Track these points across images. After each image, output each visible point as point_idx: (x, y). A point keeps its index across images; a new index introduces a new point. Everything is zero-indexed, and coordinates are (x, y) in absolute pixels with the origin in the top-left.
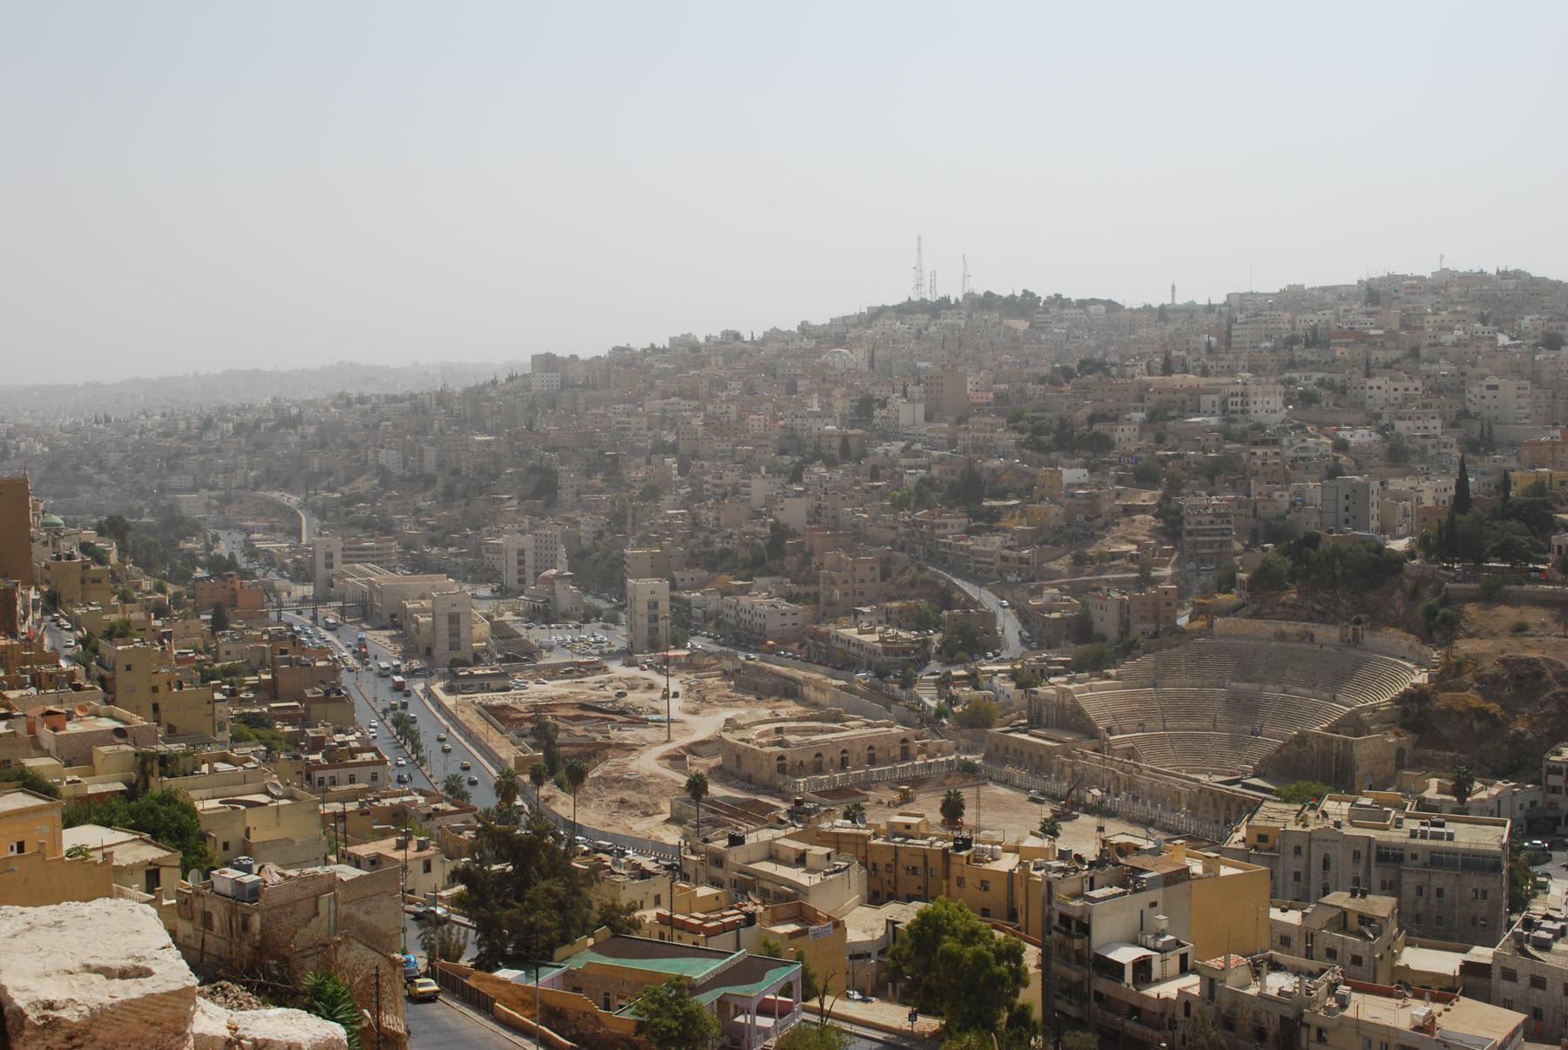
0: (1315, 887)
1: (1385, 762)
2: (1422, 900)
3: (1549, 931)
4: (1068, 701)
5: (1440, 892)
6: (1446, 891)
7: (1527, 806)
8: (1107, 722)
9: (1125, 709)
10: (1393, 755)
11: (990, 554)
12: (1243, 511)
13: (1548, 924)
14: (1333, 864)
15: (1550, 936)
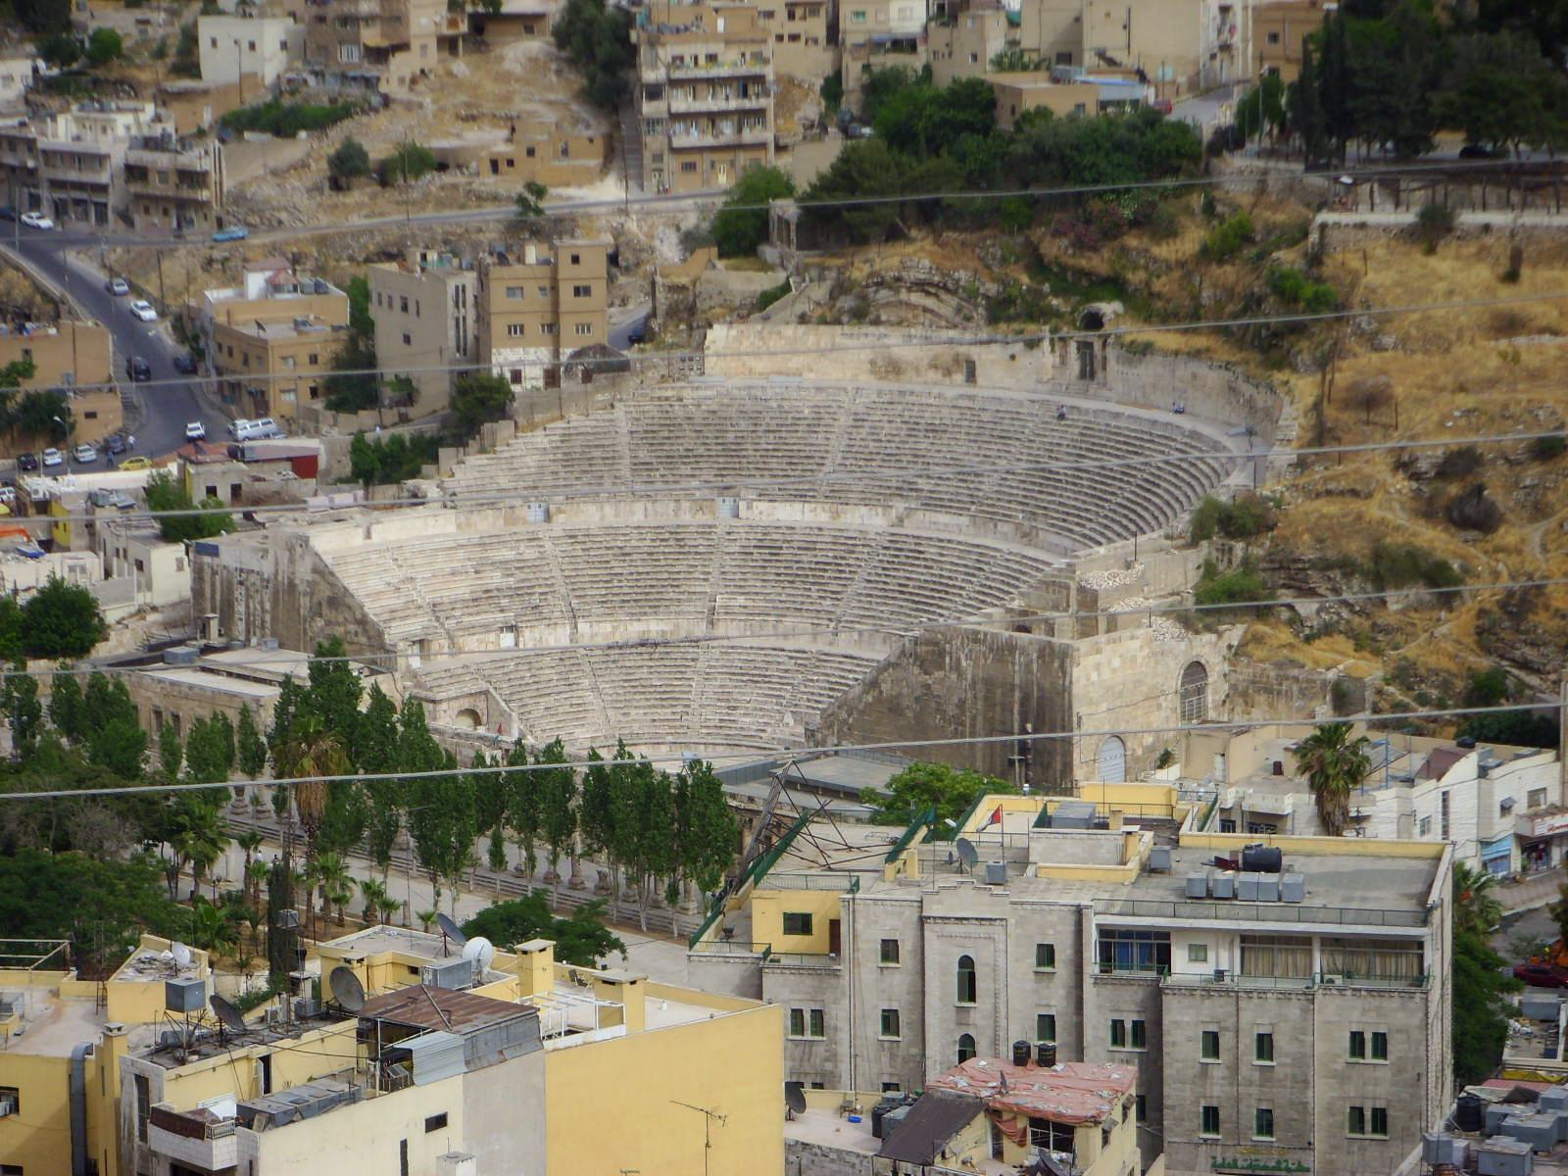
0: (940, 1046)
1: (1153, 697)
2: (1219, 1068)
3: (1522, 1134)
4: (303, 572)
5: (1265, 1045)
6: (1280, 1042)
7: (1521, 807)
8: (415, 626)
9: (463, 588)
10: (1174, 682)
11: (100, 159)
12: (796, 27)
13: (1522, 1115)
14: (981, 985)
15: (1525, 1148)
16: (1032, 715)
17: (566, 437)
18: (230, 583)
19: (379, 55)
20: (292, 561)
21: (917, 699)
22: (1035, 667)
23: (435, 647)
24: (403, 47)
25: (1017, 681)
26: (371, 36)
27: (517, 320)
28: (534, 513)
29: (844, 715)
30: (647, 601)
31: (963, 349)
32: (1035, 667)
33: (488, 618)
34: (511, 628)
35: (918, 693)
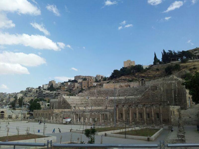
8: (74, 105)
9: (80, 103)
16: (177, 93)
17: (90, 92)
18: (53, 103)
19: (73, 87)
20: (60, 99)
21: (152, 95)
22: (177, 85)
23: (76, 107)
24: (75, 87)
25: (173, 88)
26: (72, 86)
27: (85, 86)
28: (87, 98)
29: (138, 101)
30: (99, 105)
31: (129, 84)
32: (177, 85)
33: (83, 106)
34: (85, 107)
35: (153, 95)
